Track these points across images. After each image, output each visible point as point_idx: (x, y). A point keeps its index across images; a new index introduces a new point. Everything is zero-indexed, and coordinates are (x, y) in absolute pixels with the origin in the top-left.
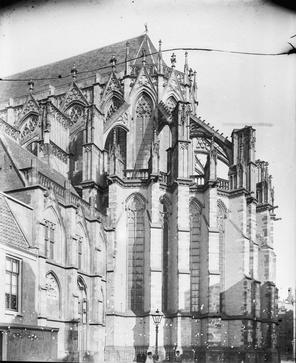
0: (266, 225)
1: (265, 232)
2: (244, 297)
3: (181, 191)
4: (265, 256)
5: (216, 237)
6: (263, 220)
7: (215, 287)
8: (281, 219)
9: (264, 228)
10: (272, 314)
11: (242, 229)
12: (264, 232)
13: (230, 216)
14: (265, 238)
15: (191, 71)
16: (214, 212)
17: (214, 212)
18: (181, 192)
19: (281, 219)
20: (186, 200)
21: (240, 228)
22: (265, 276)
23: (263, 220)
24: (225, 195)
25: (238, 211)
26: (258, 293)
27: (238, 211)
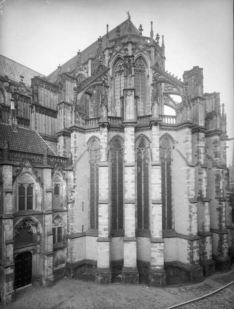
0: (215, 148)
2: (189, 219)
3: (127, 132)
5: (159, 170)
7: (157, 215)
10: (223, 226)
11: (188, 158)
12: (214, 154)
16: (157, 147)
17: (157, 147)
18: (127, 133)
20: (132, 139)
21: (185, 156)
22: (216, 192)
23: (213, 143)
24: (172, 129)
25: (184, 142)
27: (184, 142)
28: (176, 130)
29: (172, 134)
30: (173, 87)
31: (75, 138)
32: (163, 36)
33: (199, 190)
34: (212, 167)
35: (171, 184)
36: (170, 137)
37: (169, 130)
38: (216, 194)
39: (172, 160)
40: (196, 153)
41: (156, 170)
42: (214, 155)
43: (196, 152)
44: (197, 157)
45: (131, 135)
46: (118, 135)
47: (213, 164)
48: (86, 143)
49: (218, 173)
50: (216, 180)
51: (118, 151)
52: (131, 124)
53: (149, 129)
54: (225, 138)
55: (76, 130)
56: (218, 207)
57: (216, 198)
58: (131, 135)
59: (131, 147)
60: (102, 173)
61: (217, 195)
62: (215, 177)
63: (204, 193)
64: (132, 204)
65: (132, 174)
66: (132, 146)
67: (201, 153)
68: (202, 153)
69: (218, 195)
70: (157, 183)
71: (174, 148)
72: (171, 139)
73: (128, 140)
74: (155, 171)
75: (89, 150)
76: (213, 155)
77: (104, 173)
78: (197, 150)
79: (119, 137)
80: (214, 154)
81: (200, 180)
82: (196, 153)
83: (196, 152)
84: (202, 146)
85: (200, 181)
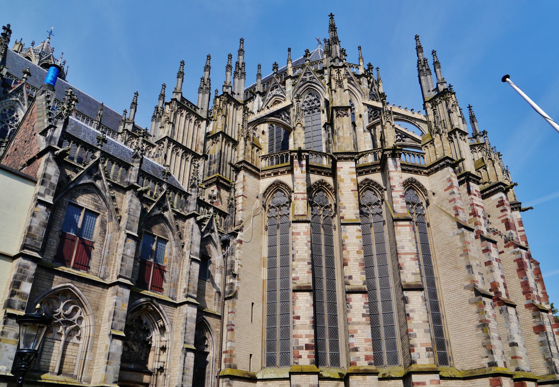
1: (505, 224)
3: (342, 168)
4: (515, 261)
5: (408, 228)
6: (498, 206)
8: (531, 208)
9: (503, 218)
13: (433, 201)
14: (509, 231)
15: (369, 65)
18: (341, 169)
19: (531, 208)
22: (523, 294)
23: (498, 206)
24: (421, 172)
25: (445, 190)
26: (516, 324)
28: (428, 174)
29: (422, 179)
30: (404, 136)
31: (244, 180)
32: (377, 68)
33: (491, 284)
34: (505, 247)
35: (433, 270)
36: (419, 184)
37: (416, 172)
38: (524, 297)
39: (428, 225)
40: (470, 216)
41: (403, 228)
42: (504, 226)
43: (470, 214)
44: (473, 223)
45: (351, 173)
46: (322, 180)
47: (506, 242)
48: (262, 195)
49: (518, 256)
50: (518, 271)
51: (323, 208)
52: (349, 156)
53: (378, 170)
54: (516, 206)
55: (246, 170)
56: (535, 325)
57: (528, 306)
58: (351, 173)
59: (352, 192)
60: (298, 234)
61: (527, 299)
62: (515, 266)
63: (501, 289)
64: (361, 295)
65: (357, 237)
66: (352, 191)
67: (479, 217)
68: (481, 217)
69: (530, 299)
70: (410, 252)
71: (428, 204)
72: (420, 188)
73: (345, 181)
74: (402, 230)
75: (267, 207)
76: (502, 228)
77: (302, 234)
78: (471, 212)
79: (325, 183)
80: (503, 225)
81: (488, 263)
82: (470, 216)
83: (470, 214)
84: (478, 204)
85: (489, 266)
